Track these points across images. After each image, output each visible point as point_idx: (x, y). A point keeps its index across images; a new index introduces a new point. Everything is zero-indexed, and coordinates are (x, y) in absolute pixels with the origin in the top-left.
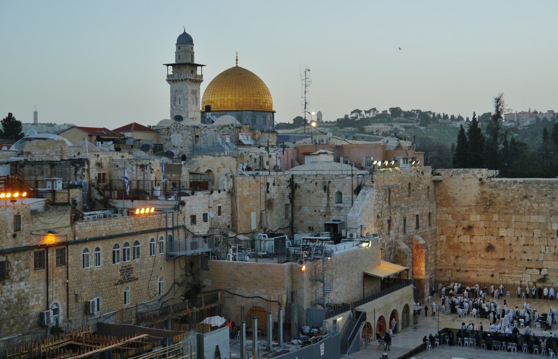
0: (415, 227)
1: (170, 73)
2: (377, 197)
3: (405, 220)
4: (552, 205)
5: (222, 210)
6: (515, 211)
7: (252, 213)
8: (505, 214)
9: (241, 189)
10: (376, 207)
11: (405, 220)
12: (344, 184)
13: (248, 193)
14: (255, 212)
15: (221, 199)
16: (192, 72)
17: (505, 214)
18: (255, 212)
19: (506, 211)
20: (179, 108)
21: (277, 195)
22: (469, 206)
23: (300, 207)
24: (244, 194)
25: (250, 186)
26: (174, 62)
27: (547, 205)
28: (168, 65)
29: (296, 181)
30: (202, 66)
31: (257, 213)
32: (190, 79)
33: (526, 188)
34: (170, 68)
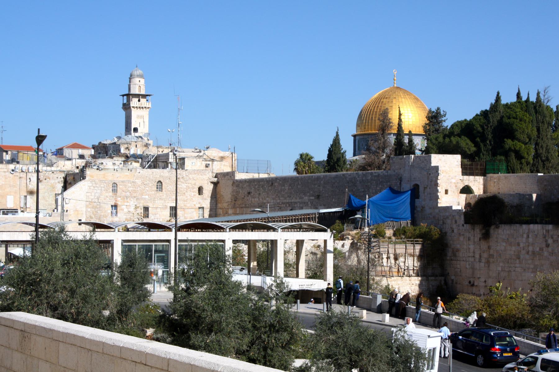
1: (125, 101)
2: (92, 188)
4: (259, 200)
6: (246, 205)
8: (242, 208)
10: (88, 194)
14: (12, 196)
16: (139, 101)
17: (242, 208)
18: (12, 196)
19: (241, 206)
22: (228, 202)
25: (6, 178)
26: (127, 93)
27: (257, 199)
28: (123, 96)
30: (149, 95)
33: (249, 186)
34: (125, 97)
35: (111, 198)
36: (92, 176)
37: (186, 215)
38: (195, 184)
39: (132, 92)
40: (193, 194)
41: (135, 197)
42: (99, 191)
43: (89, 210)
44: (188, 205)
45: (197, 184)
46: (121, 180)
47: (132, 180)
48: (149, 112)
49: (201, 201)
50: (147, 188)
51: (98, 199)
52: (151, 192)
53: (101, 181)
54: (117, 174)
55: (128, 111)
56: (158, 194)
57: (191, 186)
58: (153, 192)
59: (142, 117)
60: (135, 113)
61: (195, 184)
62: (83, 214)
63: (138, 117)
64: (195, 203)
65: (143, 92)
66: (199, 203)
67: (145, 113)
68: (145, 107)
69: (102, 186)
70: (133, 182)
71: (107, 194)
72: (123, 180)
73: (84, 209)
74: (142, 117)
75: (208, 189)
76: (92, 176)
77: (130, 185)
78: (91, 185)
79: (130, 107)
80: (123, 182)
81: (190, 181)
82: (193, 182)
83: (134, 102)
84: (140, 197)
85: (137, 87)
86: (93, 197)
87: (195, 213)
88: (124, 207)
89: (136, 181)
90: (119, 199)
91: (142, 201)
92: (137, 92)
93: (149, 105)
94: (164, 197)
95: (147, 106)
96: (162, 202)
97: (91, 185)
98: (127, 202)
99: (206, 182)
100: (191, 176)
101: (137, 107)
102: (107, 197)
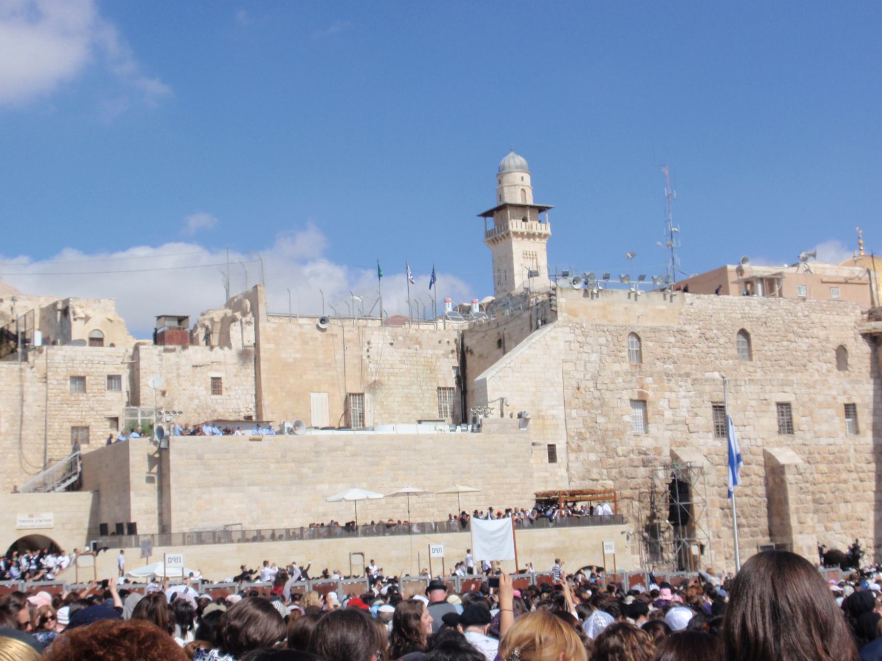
0: (777, 428)
3: (719, 408)
5: (225, 384)
7: (313, 395)
9: (272, 346)
10: (568, 367)
11: (719, 408)
12: (522, 329)
13: (298, 356)
14: (325, 395)
15: (219, 363)
18: (325, 395)
20: (504, 287)
21: (405, 367)
23: (473, 391)
24: (284, 355)
29: (468, 343)
31: (331, 397)
32: (516, 234)
35: (629, 378)
36: (572, 312)
37: (817, 428)
38: (827, 340)
39: (508, 200)
40: (825, 366)
41: (688, 375)
42: (594, 357)
43: (574, 413)
44: (820, 398)
45: (832, 339)
46: (649, 324)
47: (676, 327)
48: (547, 245)
49: (848, 387)
50: (715, 351)
51: (595, 379)
52: (724, 362)
53: (597, 327)
54: (638, 308)
55: (502, 244)
56: (742, 368)
57: (818, 346)
58: (731, 362)
59: (533, 256)
60: (518, 247)
61: (827, 340)
62: (556, 427)
63: (526, 255)
64: (834, 393)
65: (530, 202)
66: (845, 393)
67: (539, 248)
68: (540, 235)
69: (602, 340)
70: (680, 331)
71: (617, 367)
72: (654, 325)
73: (560, 412)
74: (533, 256)
75: (861, 353)
76: (572, 312)
77: (672, 339)
78: (571, 337)
79: (508, 234)
80: (654, 330)
81: (815, 331)
82: (822, 334)
83: (515, 225)
84: (699, 376)
85: (519, 192)
86: (581, 376)
87: (837, 420)
88: (663, 404)
89: (686, 327)
90: (649, 380)
91: (707, 388)
92: (519, 201)
93: (545, 229)
94: (759, 375)
95: (544, 231)
96: (755, 388)
97: (571, 337)
98: (671, 390)
99: (851, 333)
100: (815, 317)
101: (522, 234)
102: (617, 374)
